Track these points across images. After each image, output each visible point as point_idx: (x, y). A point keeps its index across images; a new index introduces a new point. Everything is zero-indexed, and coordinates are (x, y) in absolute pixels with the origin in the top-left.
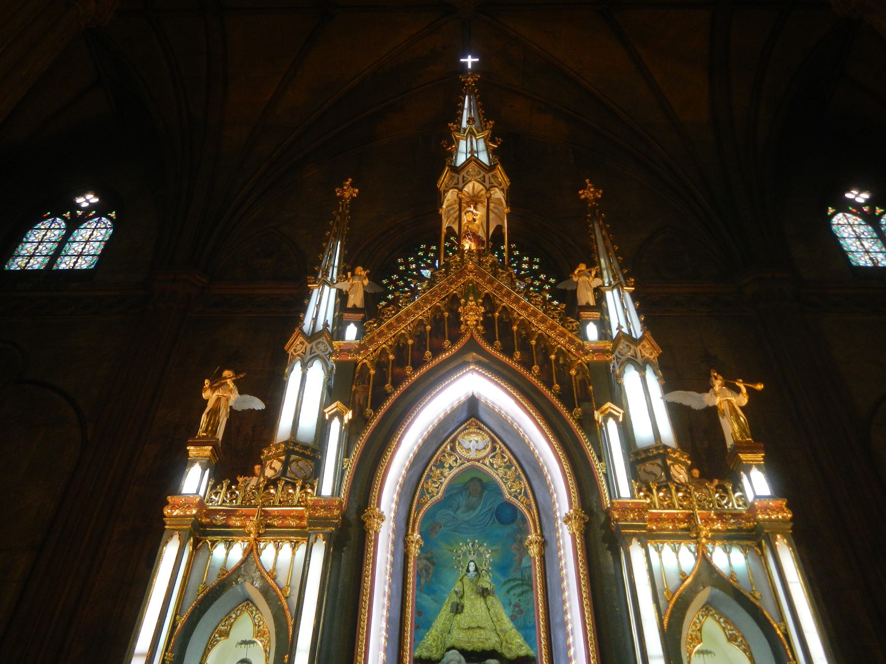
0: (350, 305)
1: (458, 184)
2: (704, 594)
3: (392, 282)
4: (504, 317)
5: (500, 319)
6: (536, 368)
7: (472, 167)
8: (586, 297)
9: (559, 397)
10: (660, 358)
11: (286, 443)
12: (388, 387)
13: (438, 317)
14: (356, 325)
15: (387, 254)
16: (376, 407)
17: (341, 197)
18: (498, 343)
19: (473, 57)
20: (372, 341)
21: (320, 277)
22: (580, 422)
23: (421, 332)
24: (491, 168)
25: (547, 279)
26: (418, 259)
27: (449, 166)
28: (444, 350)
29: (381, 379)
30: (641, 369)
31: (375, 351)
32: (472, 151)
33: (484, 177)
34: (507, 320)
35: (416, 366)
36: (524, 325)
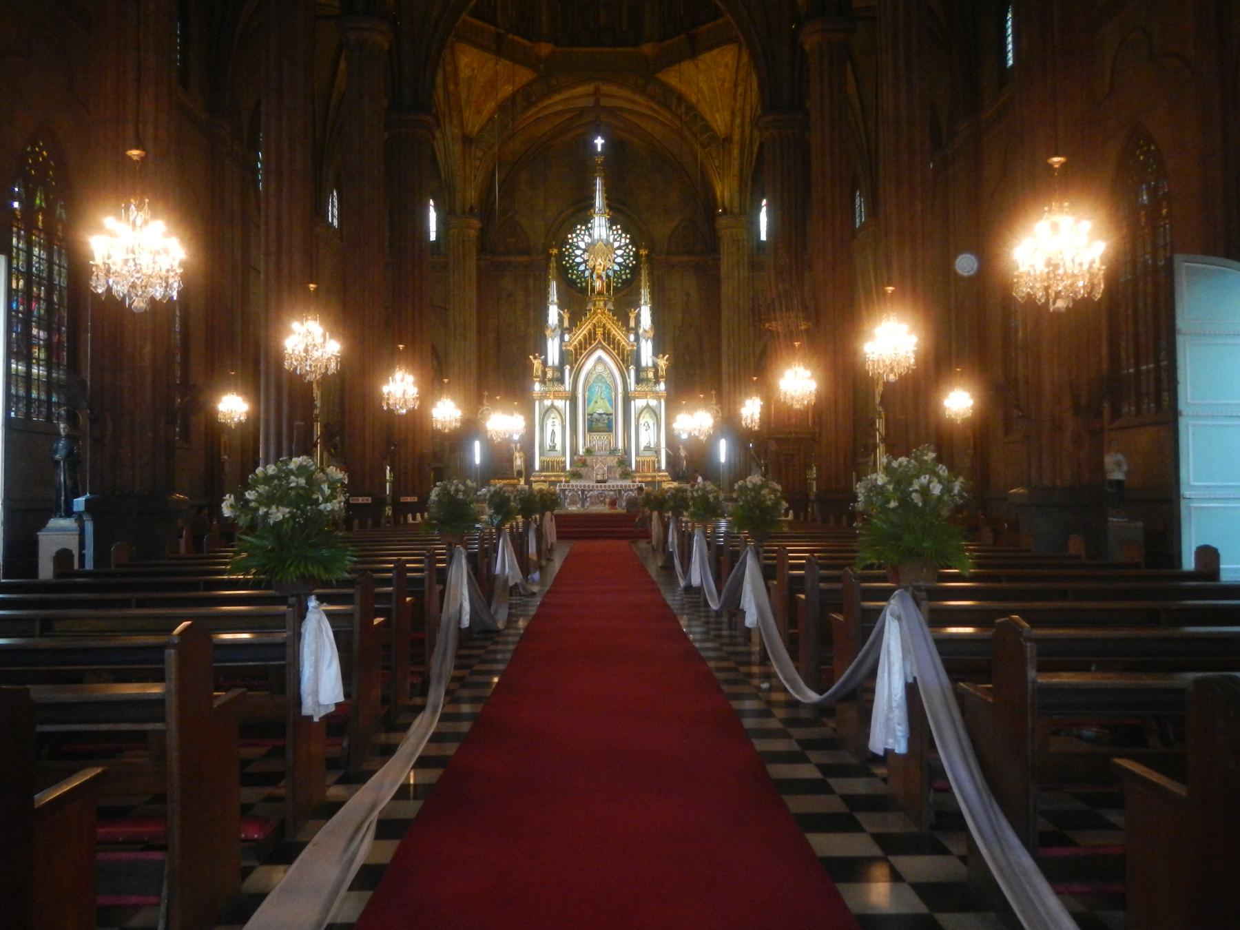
2: (646, 410)
3: (567, 250)
6: (616, 351)
8: (632, 324)
10: (654, 336)
12: (578, 357)
17: (552, 254)
18: (606, 342)
19: (602, 138)
20: (573, 341)
25: (632, 248)
26: (578, 235)
29: (576, 355)
30: (647, 341)
32: (600, 236)
35: (585, 349)
36: (614, 335)
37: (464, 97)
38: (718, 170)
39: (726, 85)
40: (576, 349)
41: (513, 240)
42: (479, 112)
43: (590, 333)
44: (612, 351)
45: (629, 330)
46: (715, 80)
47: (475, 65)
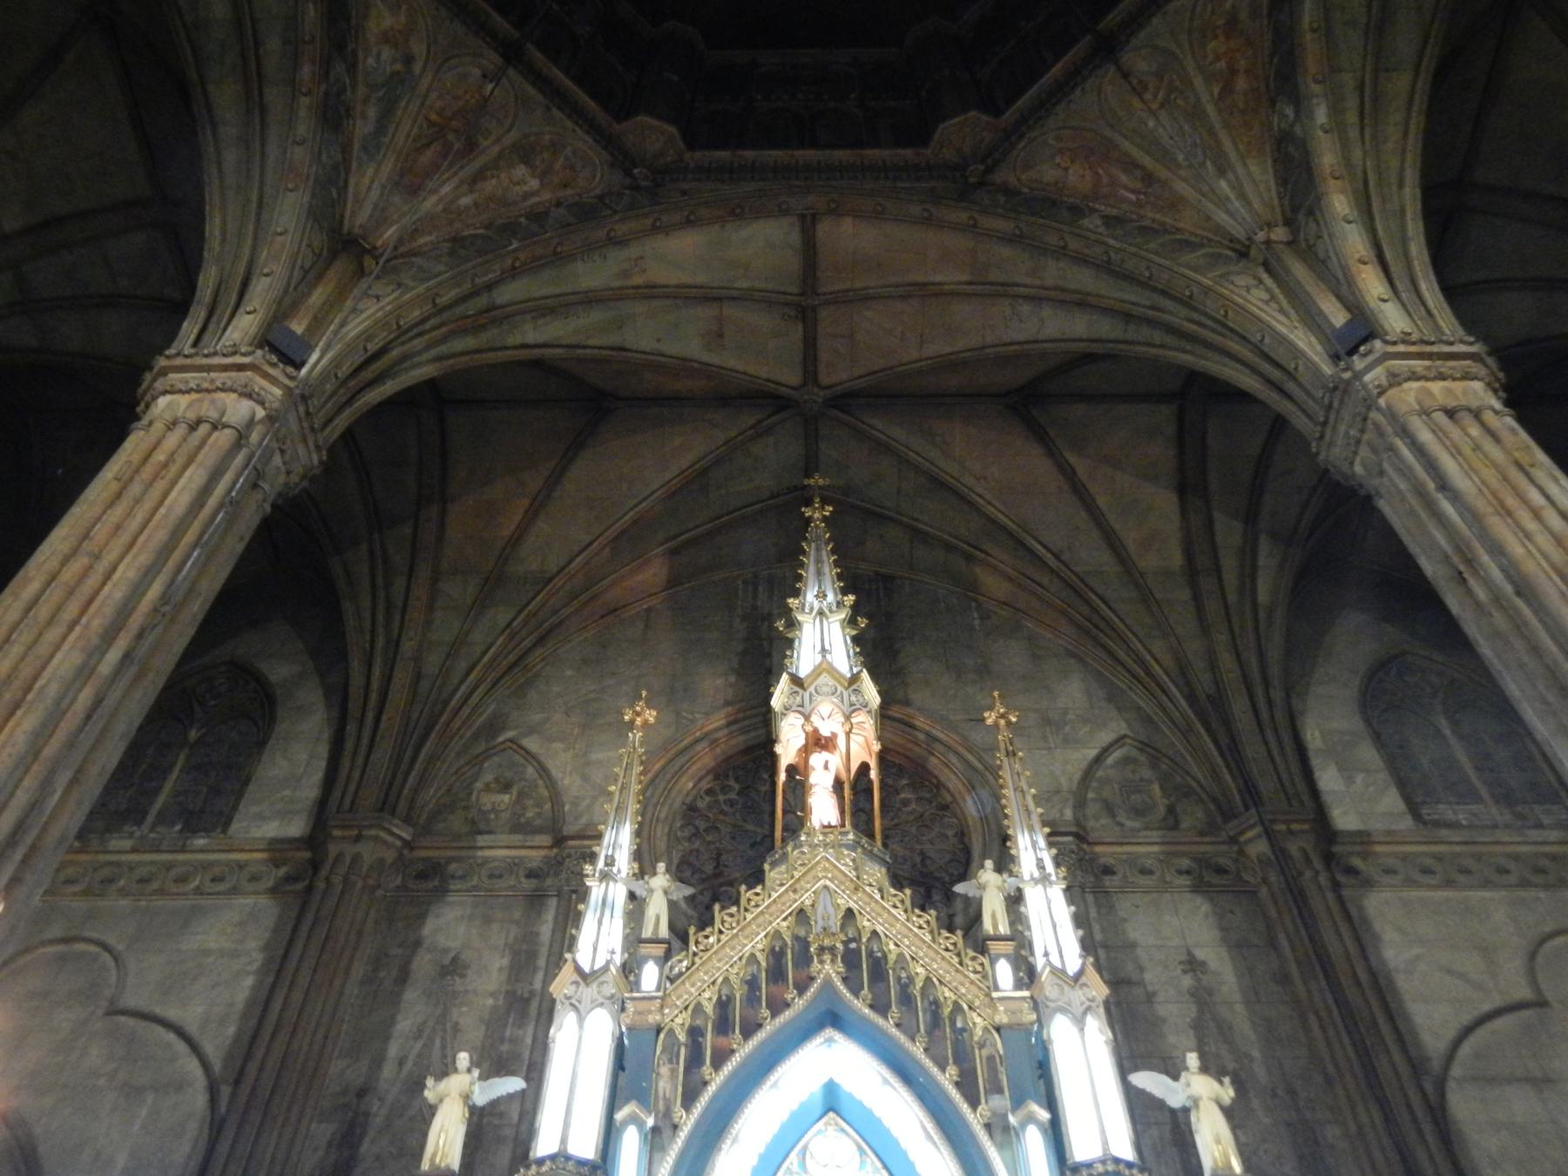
0: (647, 933)
1: (802, 706)
4: (875, 949)
5: (870, 954)
7: (824, 679)
8: (994, 916)
9: (957, 1084)
11: (553, 1158)
12: (707, 1070)
13: (777, 949)
14: (657, 963)
15: (691, 785)
16: (689, 1099)
21: (601, 864)
22: (988, 1127)
23: (753, 975)
24: (855, 679)
27: (789, 673)
28: (788, 1005)
29: (695, 1060)
30: (1080, 1022)
31: (686, 1008)
32: (823, 650)
33: (842, 694)
34: (879, 954)
35: (747, 1033)
37: (362, 127)
38: (1274, 305)
39: (1241, 84)
40: (695, 1033)
41: (506, 798)
42: (410, 183)
43: (776, 955)
44: (902, 1039)
45: (980, 944)
46: (1198, 82)
47: (418, 48)
